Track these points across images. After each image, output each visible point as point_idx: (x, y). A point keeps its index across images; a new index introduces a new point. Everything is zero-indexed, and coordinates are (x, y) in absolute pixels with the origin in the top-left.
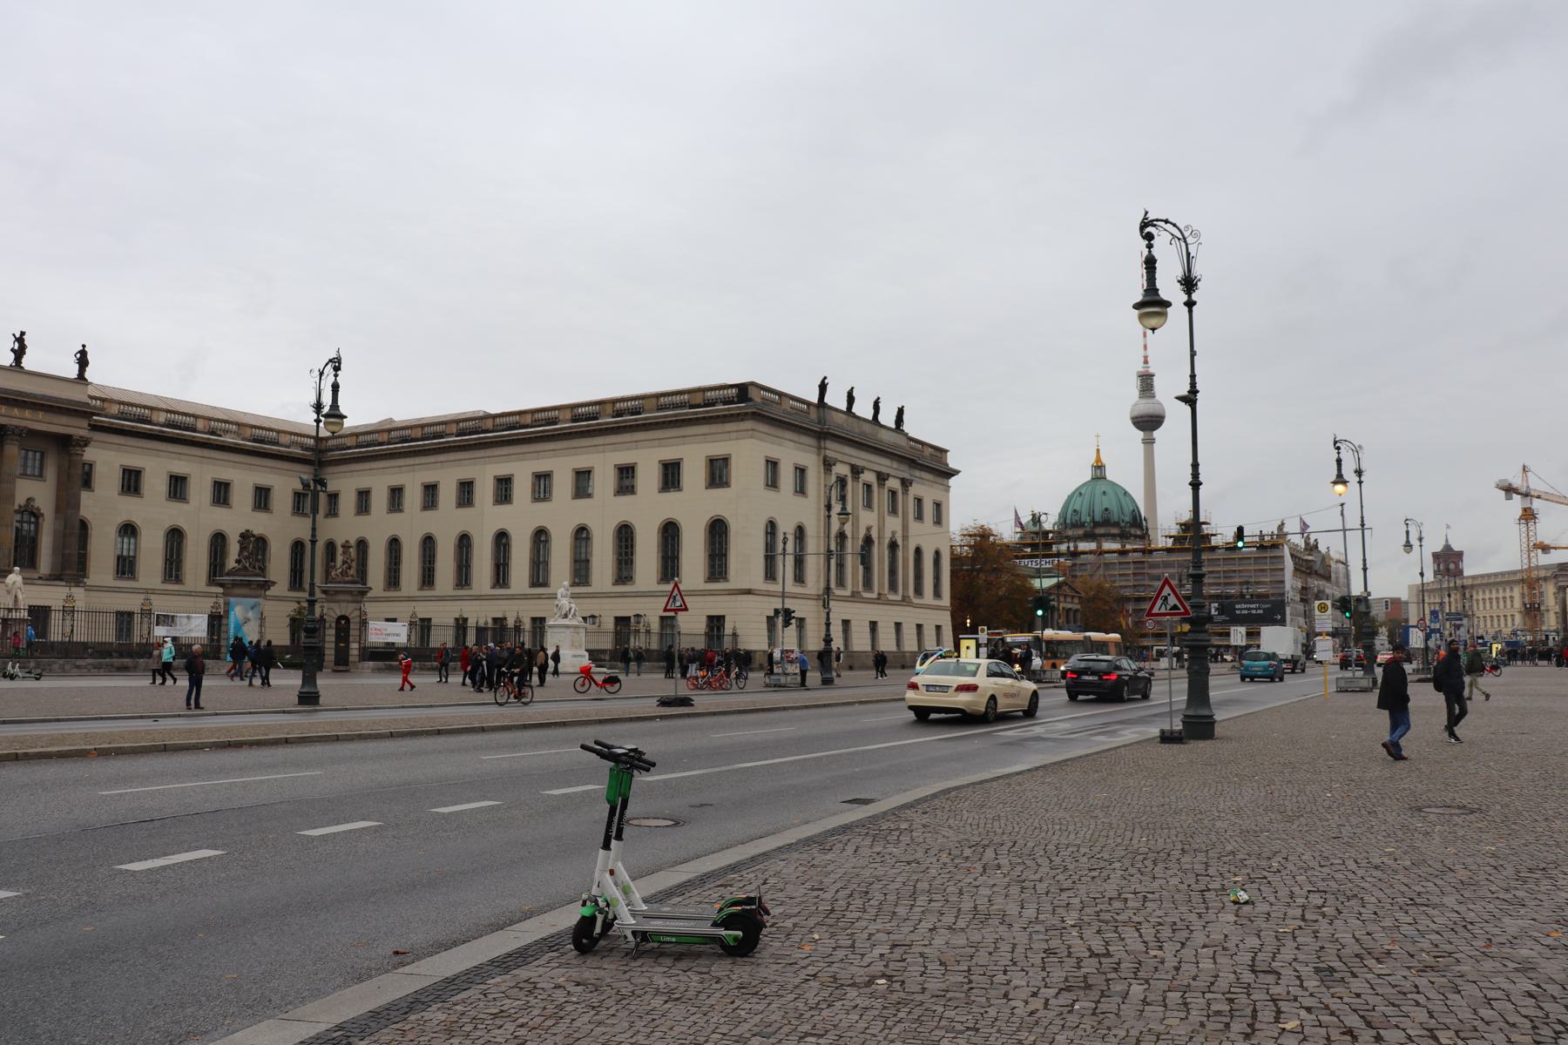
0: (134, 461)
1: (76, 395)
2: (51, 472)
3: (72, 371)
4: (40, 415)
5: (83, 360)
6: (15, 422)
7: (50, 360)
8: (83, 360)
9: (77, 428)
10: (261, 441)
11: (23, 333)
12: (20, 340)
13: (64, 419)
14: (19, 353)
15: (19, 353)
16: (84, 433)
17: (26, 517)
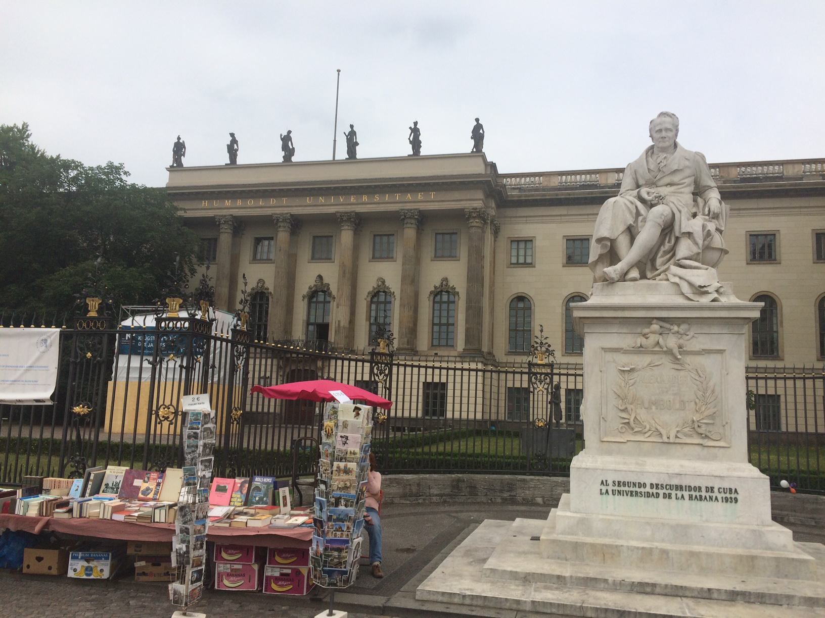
0: (577, 229)
1: (475, 168)
2: (463, 252)
3: (467, 146)
4: (432, 195)
5: (478, 135)
6: (409, 206)
7: (446, 140)
8: (478, 135)
9: (474, 201)
10: (756, 179)
11: (416, 123)
12: (415, 131)
13: (457, 195)
14: (416, 143)
15: (416, 143)
16: (478, 204)
17: (445, 298)
